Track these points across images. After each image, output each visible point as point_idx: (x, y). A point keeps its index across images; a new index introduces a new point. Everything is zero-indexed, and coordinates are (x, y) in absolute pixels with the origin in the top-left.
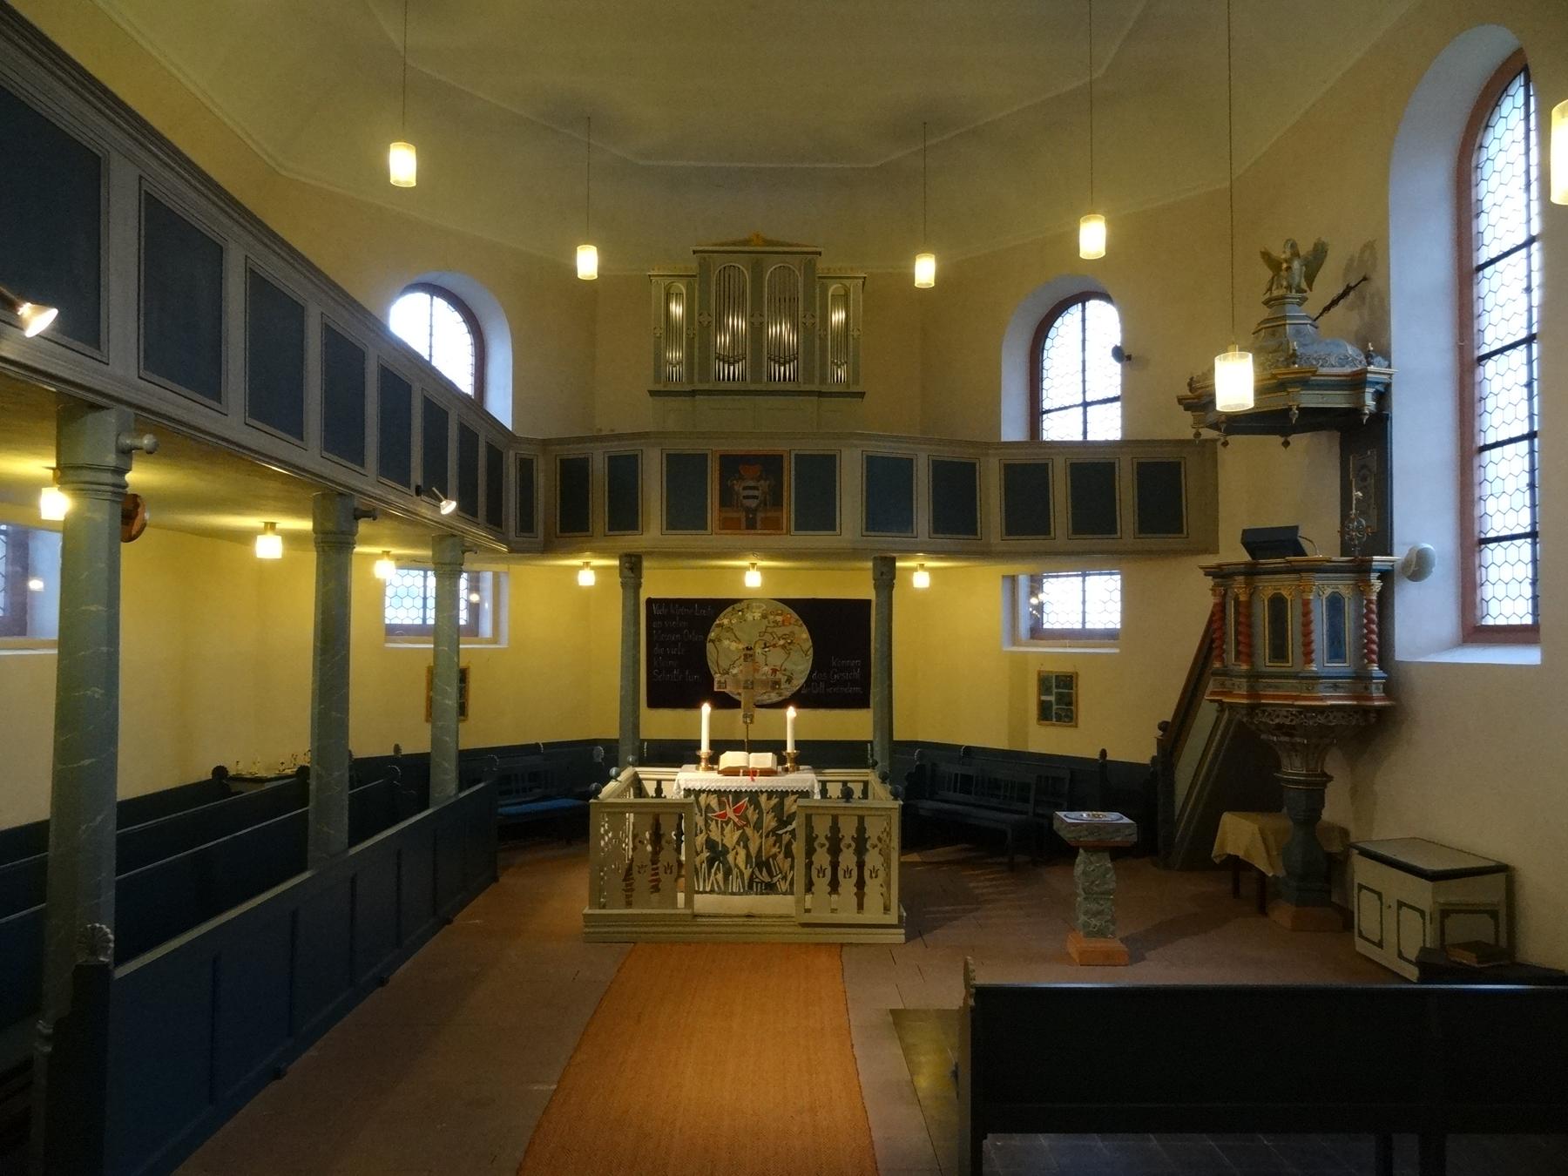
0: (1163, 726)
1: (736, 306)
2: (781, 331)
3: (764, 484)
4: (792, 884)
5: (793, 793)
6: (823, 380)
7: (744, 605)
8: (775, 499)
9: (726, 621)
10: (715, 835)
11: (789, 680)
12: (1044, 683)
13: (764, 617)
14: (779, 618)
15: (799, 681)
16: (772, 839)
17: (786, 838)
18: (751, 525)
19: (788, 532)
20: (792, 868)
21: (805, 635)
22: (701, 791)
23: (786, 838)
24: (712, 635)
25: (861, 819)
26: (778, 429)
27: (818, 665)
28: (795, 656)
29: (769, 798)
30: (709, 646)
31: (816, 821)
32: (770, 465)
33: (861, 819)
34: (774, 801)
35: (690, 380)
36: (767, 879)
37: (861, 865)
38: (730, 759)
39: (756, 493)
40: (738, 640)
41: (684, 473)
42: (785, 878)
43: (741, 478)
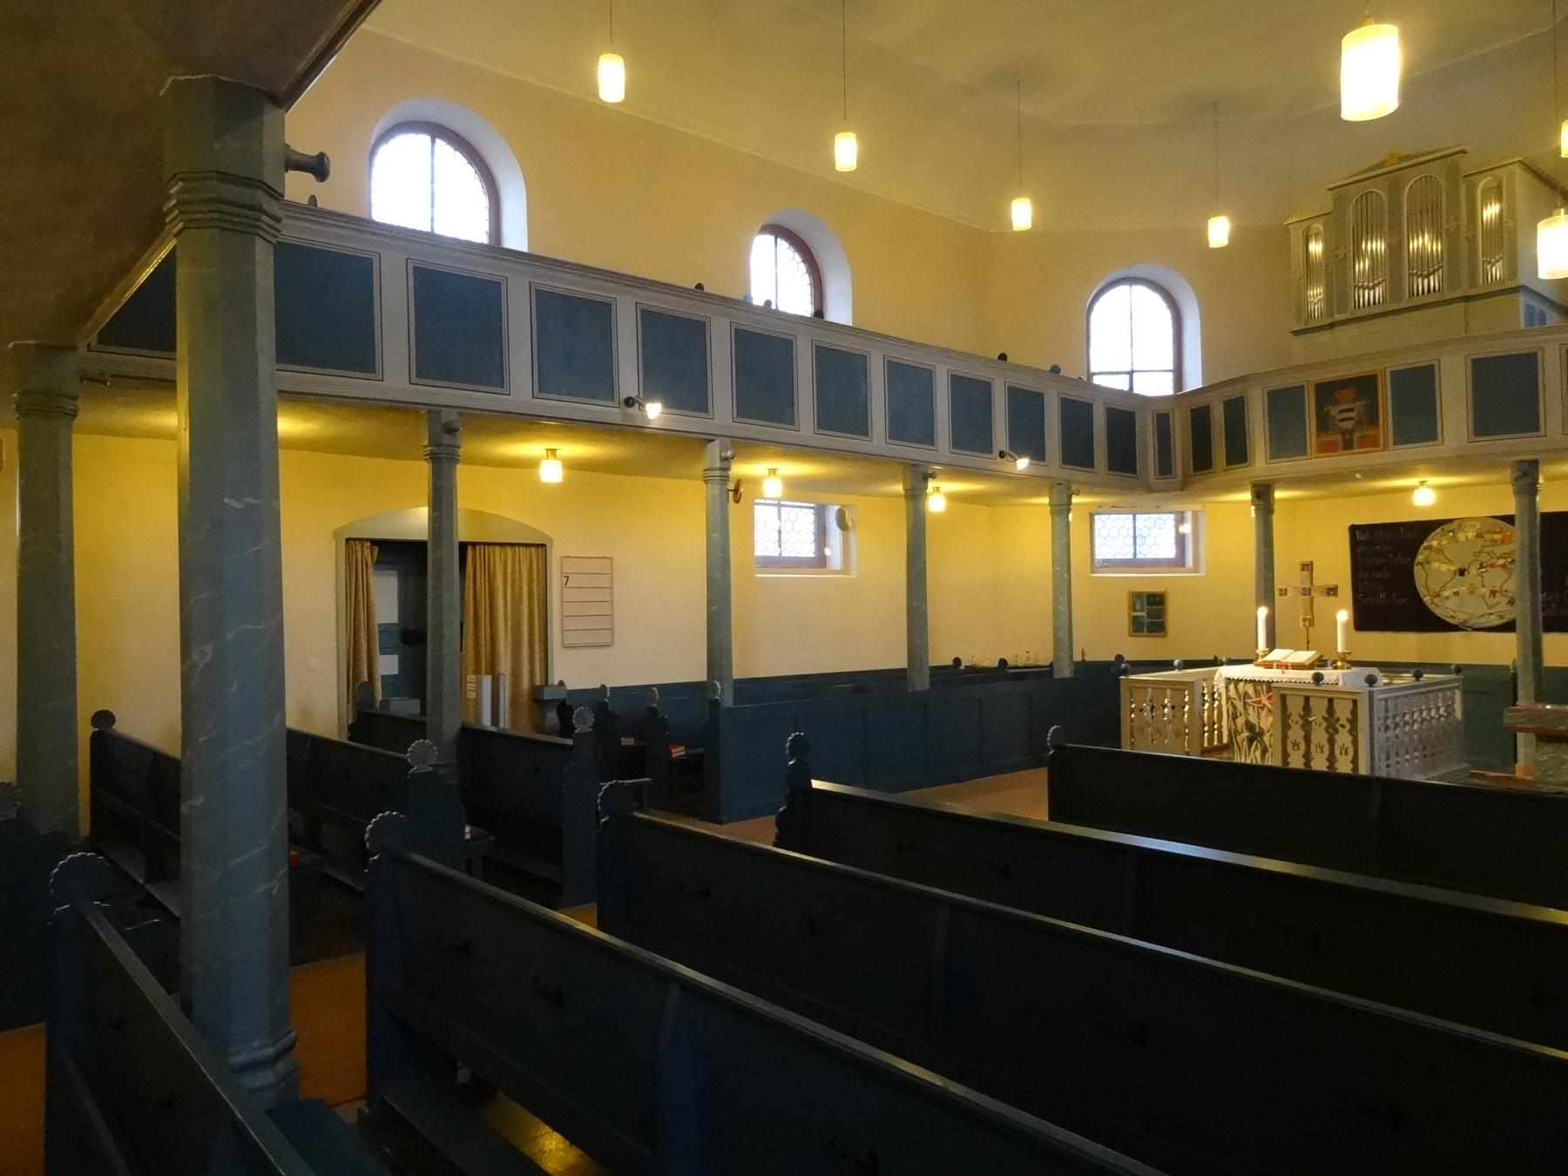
1: (1371, 234)
2: (1424, 243)
3: (1359, 405)
6: (1473, 283)
8: (1372, 417)
9: (1435, 543)
10: (1253, 719)
13: (1479, 536)
18: (1348, 445)
19: (1386, 448)
22: (1239, 681)
24: (1420, 558)
25: (1331, 701)
26: (1347, 351)
30: (1417, 569)
31: (1289, 701)
32: (1365, 386)
33: (1331, 701)
37: (1331, 741)
38: (1278, 655)
39: (1351, 414)
41: (1284, 404)
43: (1337, 403)
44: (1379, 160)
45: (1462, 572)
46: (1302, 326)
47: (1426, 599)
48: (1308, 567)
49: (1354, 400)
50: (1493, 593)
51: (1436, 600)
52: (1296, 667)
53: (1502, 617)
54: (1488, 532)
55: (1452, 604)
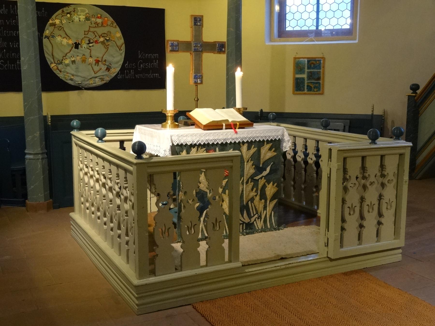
0: (415, 88)
4: (265, 221)
5: (268, 142)
7: (71, 9)
9: (57, 22)
11: (108, 69)
12: (298, 67)
13: (87, 19)
14: (99, 21)
15: (116, 69)
16: (251, 185)
17: (261, 183)
20: (265, 208)
21: (119, 34)
22: (192, 146)
23: (261, 183)
27: (130, 56)
28: (112, 50)
29: (249, 148)
34: (253, 150)
36: (247, 220)
40: (68, 36)
42: (260, 217)
45: (77, 46)
47: (52, 66)
48: (197, 21)
50: (97, 62)
51: (60, 67)
52: (231, 126)
53: (102, 79)
54: (93, 16)
55: (71, 70)
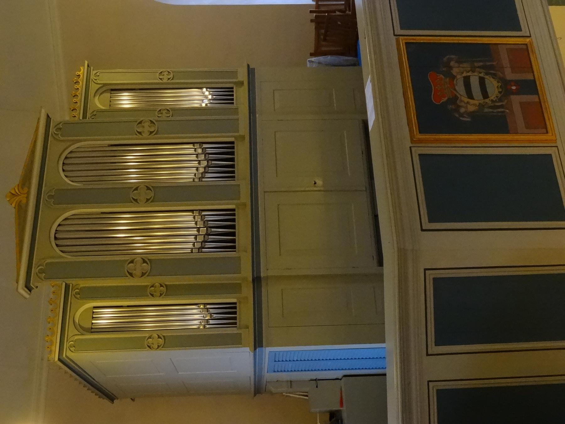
18: (531, 87)
35: (235, 288)
43: (454, 99)
44: (11, 210)
46: (249, 335)
49: (453, 77)
